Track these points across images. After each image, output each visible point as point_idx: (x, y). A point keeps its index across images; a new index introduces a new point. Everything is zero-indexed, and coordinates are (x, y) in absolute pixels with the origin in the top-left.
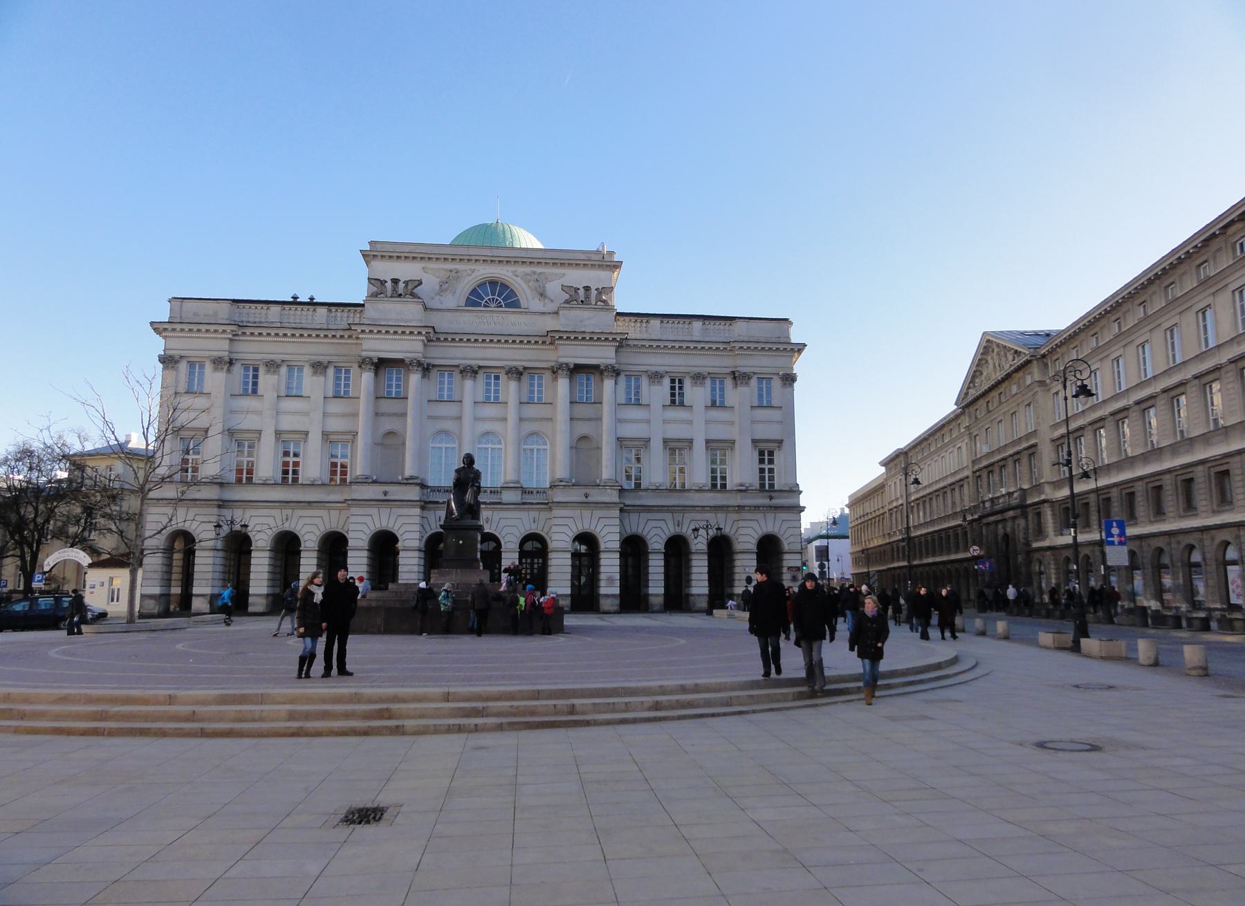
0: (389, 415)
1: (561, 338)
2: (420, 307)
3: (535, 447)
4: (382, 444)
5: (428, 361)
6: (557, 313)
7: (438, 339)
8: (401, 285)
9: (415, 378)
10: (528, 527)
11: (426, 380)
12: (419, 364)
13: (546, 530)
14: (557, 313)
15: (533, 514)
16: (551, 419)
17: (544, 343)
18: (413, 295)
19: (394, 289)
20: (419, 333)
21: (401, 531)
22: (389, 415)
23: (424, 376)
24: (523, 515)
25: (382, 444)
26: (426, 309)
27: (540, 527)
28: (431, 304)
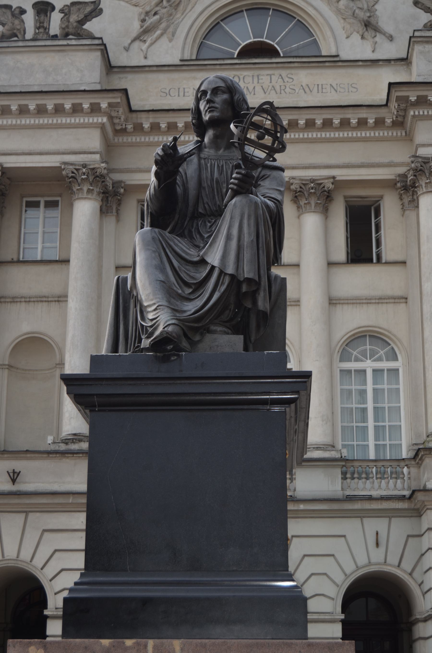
0: (28, 300)
1: (422, 101)
2: (95, 57)
3: (369, 365)
4: (10, 367)
5: (117, 177)
6: (405, 61)
7: (138, 128)
8: (56, 18)
9: (85, 209)
10: (362, 560)
11: (110, 222)
12: (96, 178)
13: (407, 565)
14: (405, 61)
15: (374, 525)
16: (405, 299)
17: (379, 123)
18: (80, 34)
19: (42, 27)
20: (95, 109)
21: (50, 571)
22: (28, 300)
23: (104, 211)
24: (350, 527)
25: (10, 367)
26: (110, 68)
27: (393, 559)
28: (118, 58)
